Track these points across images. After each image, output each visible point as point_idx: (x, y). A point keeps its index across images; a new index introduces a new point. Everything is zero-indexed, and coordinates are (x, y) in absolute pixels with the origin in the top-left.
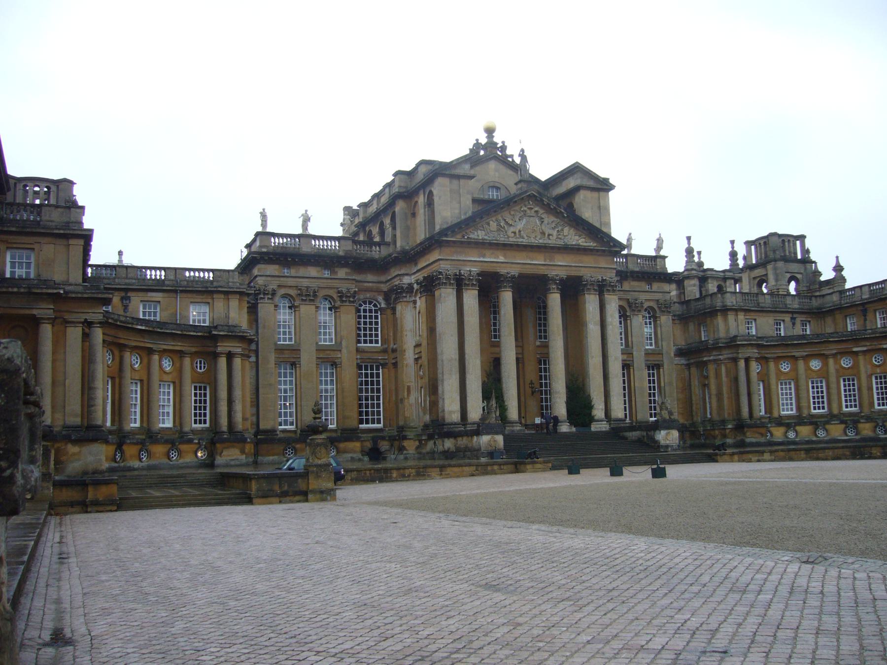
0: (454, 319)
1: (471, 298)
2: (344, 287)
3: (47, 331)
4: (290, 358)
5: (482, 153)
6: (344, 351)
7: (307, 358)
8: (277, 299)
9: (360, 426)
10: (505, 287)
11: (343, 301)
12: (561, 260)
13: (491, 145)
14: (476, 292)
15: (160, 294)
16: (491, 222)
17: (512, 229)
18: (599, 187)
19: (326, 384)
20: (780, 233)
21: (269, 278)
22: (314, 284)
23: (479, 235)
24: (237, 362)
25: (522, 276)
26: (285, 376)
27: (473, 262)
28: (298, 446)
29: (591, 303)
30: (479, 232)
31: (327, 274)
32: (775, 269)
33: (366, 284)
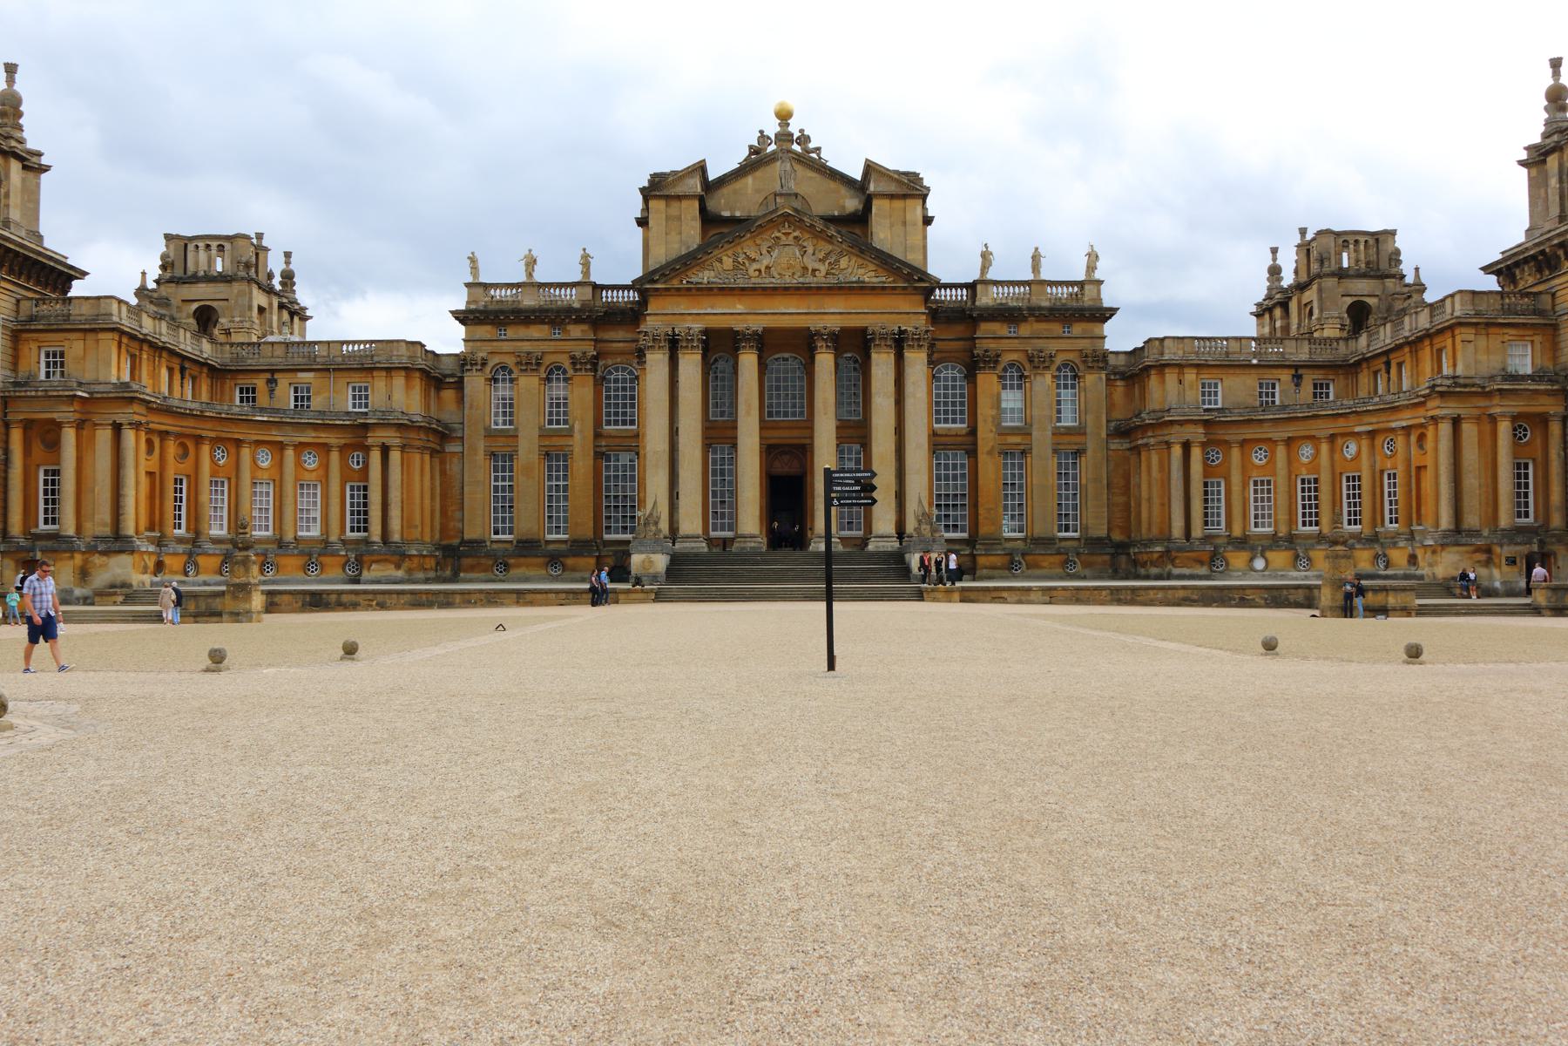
0: (665, 396)
1: (690, 365)
3: (69, 436)
5: (773, 147)
6: (577, 436)
7: (528, 449)
8: (488, 369)
11: (576, 370)
12: (836, 305)
13: (784, 137)
14: (699, 357)
15: (311, 375)
17: (755, 266)
19: (558, 479)
20: (1336, 229)
23: (705, 276)
24: (395, 456)
27: (694, 316)
28: (512, 561)
29: (882, 364)
32: (1320, 290)
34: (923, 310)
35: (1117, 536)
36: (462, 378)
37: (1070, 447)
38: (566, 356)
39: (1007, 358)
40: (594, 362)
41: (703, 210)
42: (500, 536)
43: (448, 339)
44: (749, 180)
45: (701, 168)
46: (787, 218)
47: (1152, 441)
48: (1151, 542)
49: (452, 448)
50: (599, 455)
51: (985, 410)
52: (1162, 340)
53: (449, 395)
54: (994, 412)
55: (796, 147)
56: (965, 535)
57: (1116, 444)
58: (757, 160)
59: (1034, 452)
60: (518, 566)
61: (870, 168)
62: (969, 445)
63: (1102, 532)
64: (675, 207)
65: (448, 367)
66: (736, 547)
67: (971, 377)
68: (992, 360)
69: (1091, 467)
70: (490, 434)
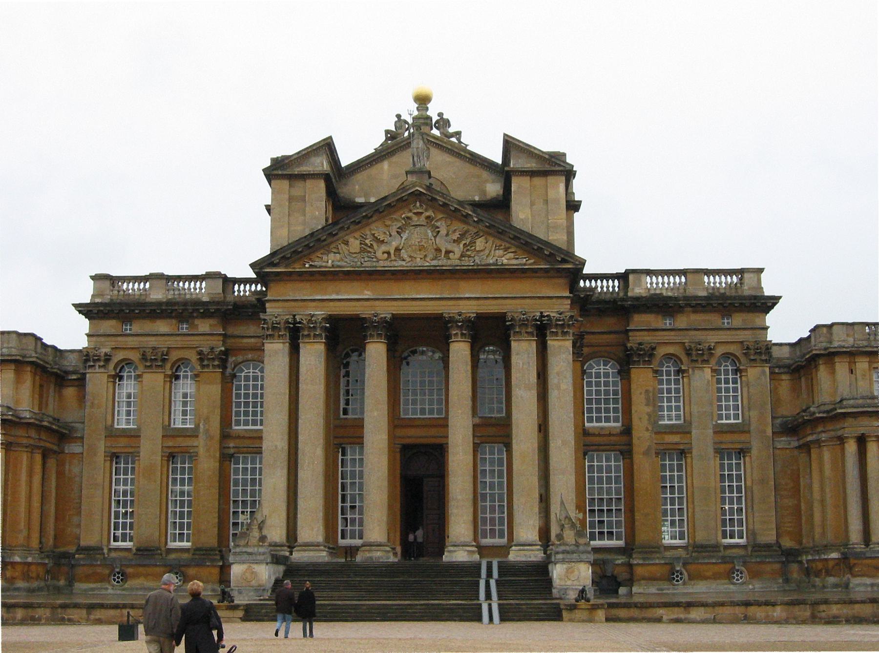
0: (283, 388)
1: (313, 356)
2: (205, 345)
4: (122, 450)
6: (202, 436)
8: (111, 366)
9: (592, 542)
10: (372, 336)
11: (203, 367)
12: (470, 289)
13: (423, 121)
16: (351, 240)
17: (384, 248)
18: (547, 167)
21: (103, 339)
22: (162, 344)
23: (329, 261)
25: (397, 319)
26: (126, 473)
28: (130, 570)
29: (523, 352)
30: (332, 255)
31: (184, 328)
33: (245, 341)
34: (567, 294)
35: (787, 543)
36: (84, 374)
37: (732, 446)
38: (194, 352)
39: (662, 351)
40: (223, 359)
41: (331, 193)
42: (120, 544)
43: (70, 334)
44: (386, 165)
45: (327, 147)
46: (422, 198)
47: (824, 436)
48: (827, 548)
49: (75, 448)
50: (226, 458)
51: (640, 408)
52: (830, 326)
53: (70, 392)
54: (649, 409)
55: (435, 132)
56: (621, 543)
57: (783, 441)
58: (394, 144)
59: (694, 452)
60: (136, 576)
61: (510, 145)
62: (623, 444)
63: (769, 537)
64: (299, 189)
65: (71, 363)
66: (359, 558)
67: (624, 373)
68: (647, 354)
69: (756, 467)
70: (112, 434)
